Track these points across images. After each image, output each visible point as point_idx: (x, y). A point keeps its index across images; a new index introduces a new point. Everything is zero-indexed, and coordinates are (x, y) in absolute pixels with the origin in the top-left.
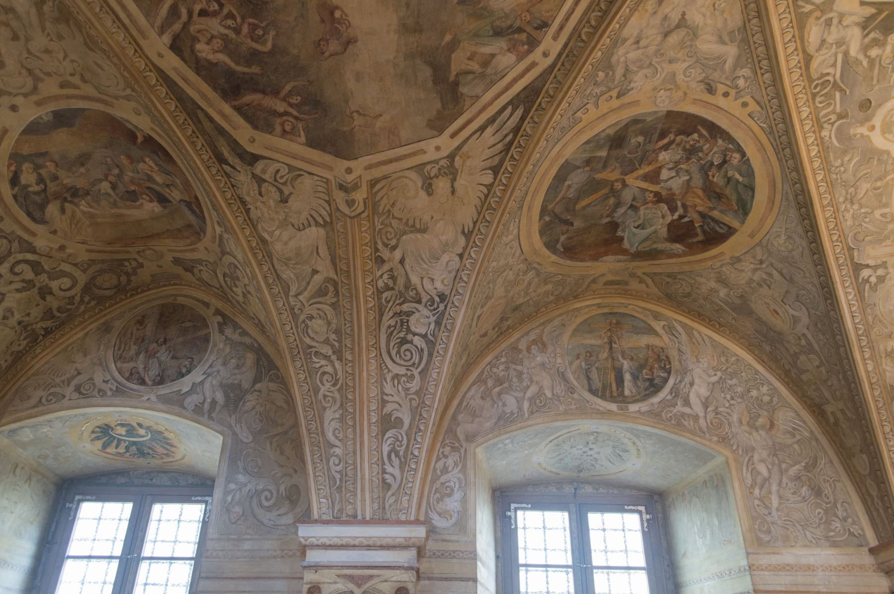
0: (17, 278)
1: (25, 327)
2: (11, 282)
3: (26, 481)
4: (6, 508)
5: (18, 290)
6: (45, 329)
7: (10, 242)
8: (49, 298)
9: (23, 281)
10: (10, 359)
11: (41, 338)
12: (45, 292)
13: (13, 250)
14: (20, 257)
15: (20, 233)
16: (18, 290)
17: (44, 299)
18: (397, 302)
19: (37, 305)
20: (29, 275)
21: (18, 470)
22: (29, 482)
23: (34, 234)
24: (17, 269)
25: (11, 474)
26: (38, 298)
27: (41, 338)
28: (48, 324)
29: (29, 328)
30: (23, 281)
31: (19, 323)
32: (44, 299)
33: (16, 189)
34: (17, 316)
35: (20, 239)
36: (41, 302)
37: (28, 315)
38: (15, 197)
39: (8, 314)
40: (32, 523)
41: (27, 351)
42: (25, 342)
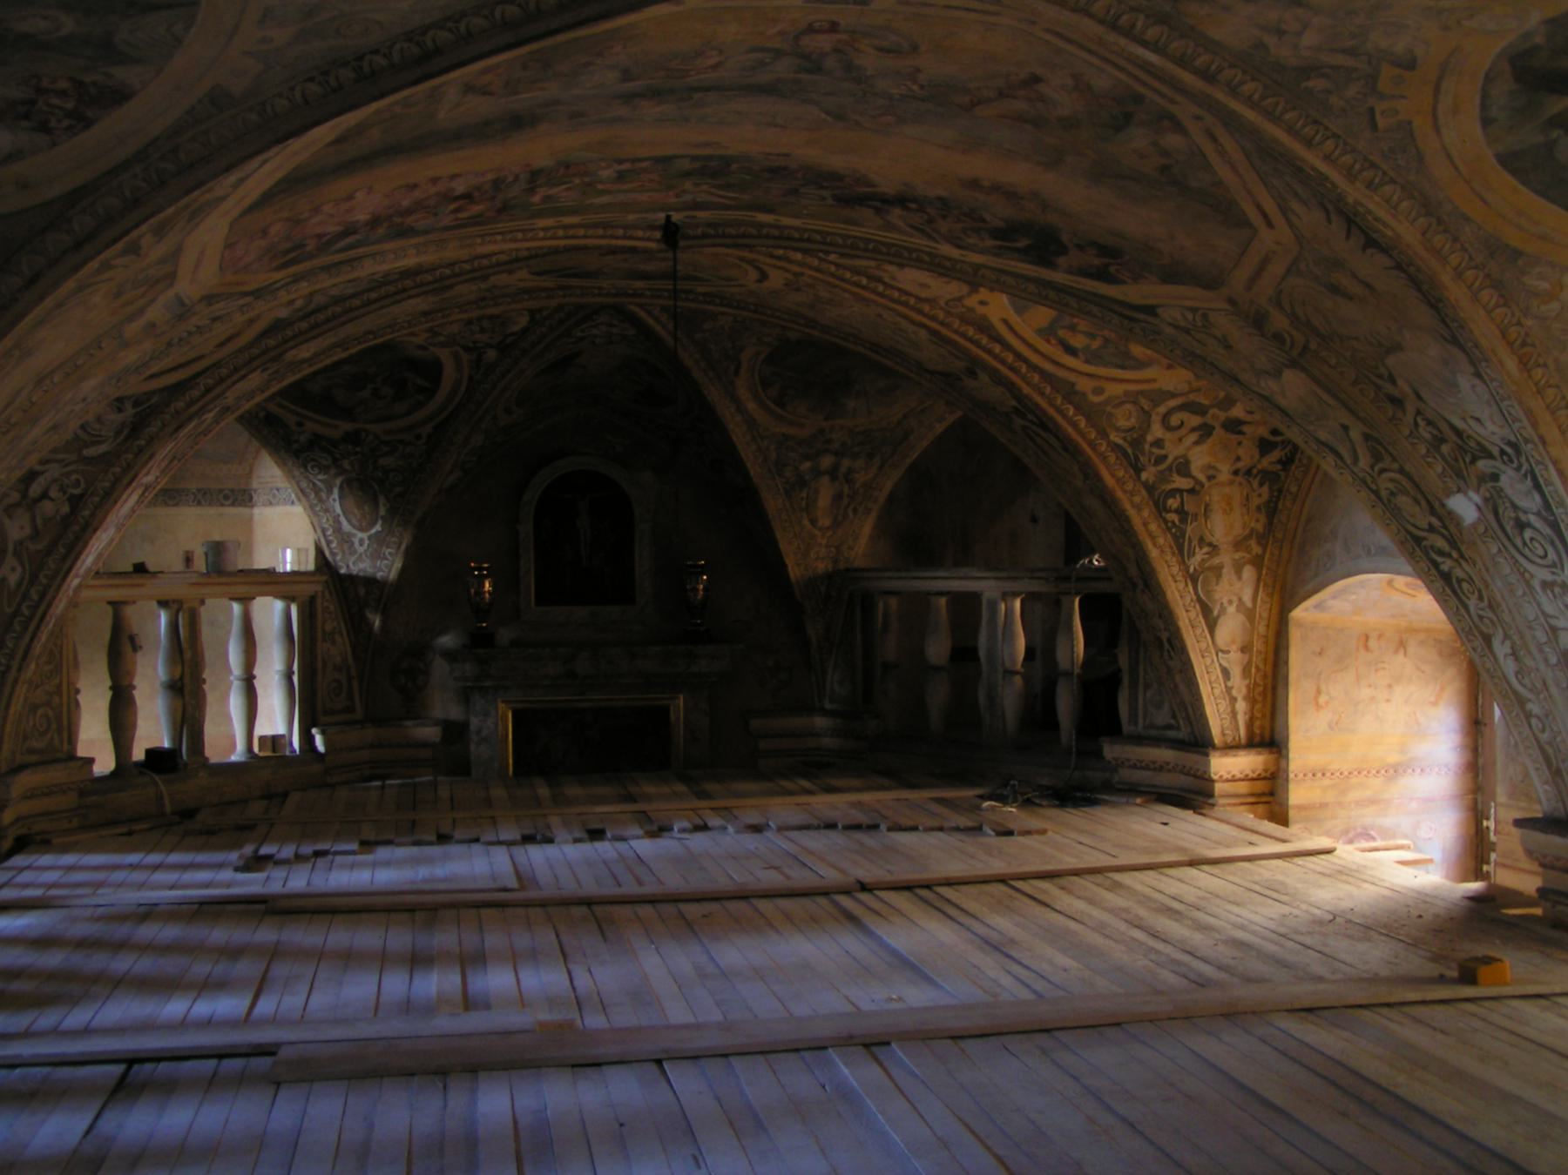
0: (1183, 431)
1: (1249, 472)
2: (1180, 440)
3: (1396, 652)
4: (1372, 699)
5: (1197, 443)
6: (1279, 462)
7: (1134, 403)
8: (1245, 429)
9: (1193, 430)
10: (1263, 518)
11: (1282, 473)
12: (1234, 426)
13: (1146, 408)
14: (1162, 409)
15: (1132, 387)
16: (1197, 443)
17: (1241, 433)
18: (1467, 460)
19: (1240, 443)
20: (1195, 421)
21: (1372, 643)
22: (1402, 651)
23: (1154, 380)
24: (1174, 420)
25: (1362, 651)
26: (1234, 437)
27: (1282, 473)
28: (1276, 455)
29: (1255, 471)
30: (1193, 430)
31: (1236, 473)
32: (1241, 433)
33: (1080, 354)
34: (1225, 472)
35: (1142, 393)
36: (1240, 437)
37: (1238, 459)
38: (1087, 361)
39: (1211, 472)
40: (1435, 704)
41: (1278, 498)
42: (1265, 489)
